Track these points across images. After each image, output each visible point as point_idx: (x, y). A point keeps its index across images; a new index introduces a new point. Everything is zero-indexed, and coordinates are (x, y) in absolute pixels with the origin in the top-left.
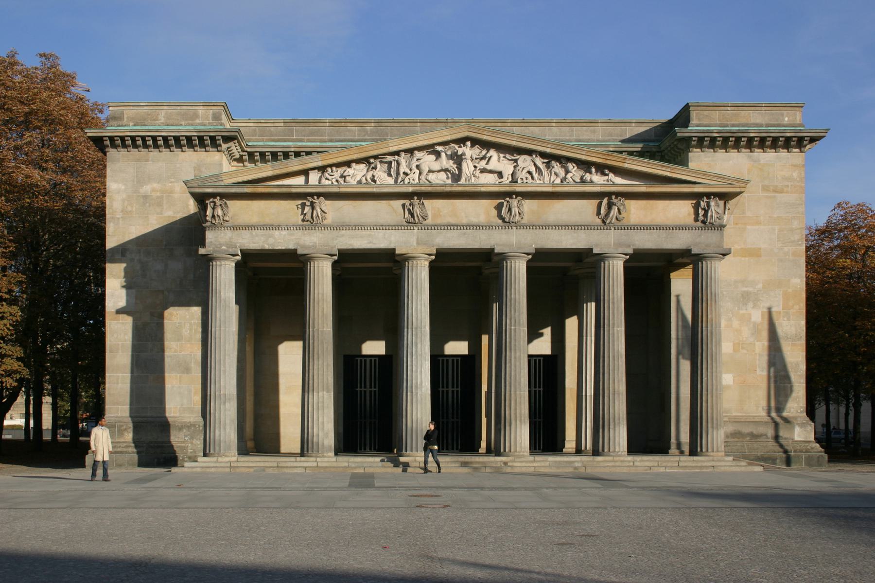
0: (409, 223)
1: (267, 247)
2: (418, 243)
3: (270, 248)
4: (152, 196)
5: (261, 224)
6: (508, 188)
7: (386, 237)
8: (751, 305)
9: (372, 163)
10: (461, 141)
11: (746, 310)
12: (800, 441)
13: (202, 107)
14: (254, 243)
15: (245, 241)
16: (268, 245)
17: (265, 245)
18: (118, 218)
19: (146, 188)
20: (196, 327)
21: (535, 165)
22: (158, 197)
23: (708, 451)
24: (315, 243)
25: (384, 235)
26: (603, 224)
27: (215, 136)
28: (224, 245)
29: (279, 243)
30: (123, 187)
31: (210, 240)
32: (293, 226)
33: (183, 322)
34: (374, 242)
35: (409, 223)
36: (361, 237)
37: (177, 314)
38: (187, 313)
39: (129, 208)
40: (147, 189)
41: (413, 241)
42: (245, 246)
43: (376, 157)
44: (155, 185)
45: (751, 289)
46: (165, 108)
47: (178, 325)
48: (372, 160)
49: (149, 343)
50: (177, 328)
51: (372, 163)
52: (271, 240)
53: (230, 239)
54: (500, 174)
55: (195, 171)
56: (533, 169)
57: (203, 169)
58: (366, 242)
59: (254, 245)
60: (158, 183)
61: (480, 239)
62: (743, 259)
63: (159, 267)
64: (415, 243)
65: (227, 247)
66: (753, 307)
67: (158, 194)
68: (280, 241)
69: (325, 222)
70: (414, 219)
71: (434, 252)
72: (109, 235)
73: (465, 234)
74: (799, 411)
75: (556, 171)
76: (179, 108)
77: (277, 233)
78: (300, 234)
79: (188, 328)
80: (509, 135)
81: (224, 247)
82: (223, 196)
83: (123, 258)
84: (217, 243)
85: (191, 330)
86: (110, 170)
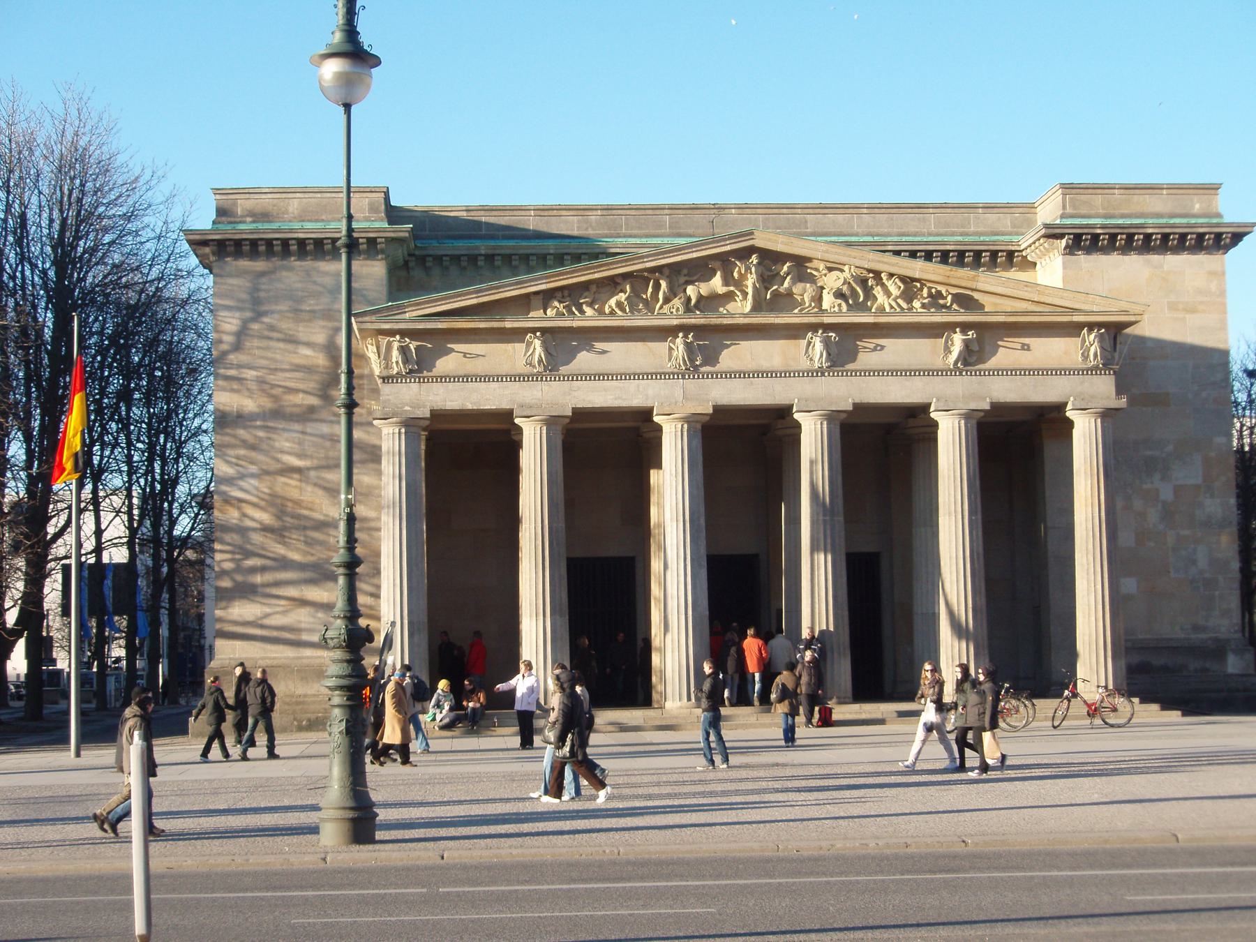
1: (470, 407)
5: (462, 373)
7: (641, 389)
8: (1157, 476)
9: (619, 284)
10: (744, 254)
11: (1152, 483)
12: (1236, 675)
14: (451, 401)
15: (438, 398)
24: (539, 399)
27: (376, 238)
28: (407, 405)
34: (624, 397)
41: (679, 394)
46: (298, 195)
48: (619, 280)
51: (619, 284)
59: (450, 403)
62: (1144, 409)
65: (411, 407)
66: (1162, 479)
71: (711, 411)
74: (1232, 631)
76: (319, 195)
78: (517, 387)
81: (407, 408)
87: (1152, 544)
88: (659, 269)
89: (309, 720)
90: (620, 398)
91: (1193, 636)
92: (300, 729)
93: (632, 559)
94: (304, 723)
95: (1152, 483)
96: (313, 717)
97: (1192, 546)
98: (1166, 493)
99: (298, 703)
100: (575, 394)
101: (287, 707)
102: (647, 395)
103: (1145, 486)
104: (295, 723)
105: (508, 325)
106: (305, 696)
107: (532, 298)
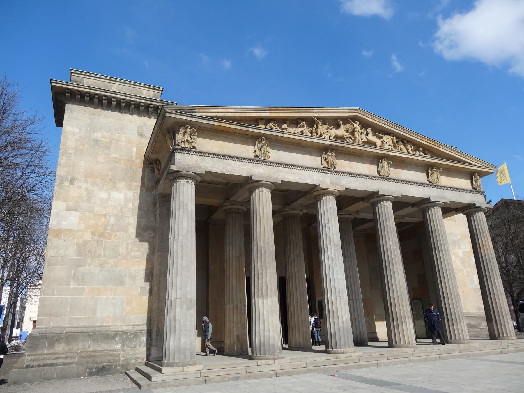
0: (325, 168)
1: (226, 172)
2: (331, 183)
3: (228, 173)
4: (102, 141)
6: (385, 152)
7: (311, 176)
8: (457, 248)
10: (354, 119)
13: (145, 89)
14: (215, 168)
16: (227, 171)
17: (225, 171)
18: (70, 154)
19: (97, 134)
20: (131, 246)
21: (393, 141)
22: (106, 142)
23: (507, 336)
24: (262, 174)
25: (309, 174)
26: (431, 184)
29: (235, 170)
30: (78, 131)
31: (179, 160)
32: (246, 159)
33: (121, 242)
35: (325, 168)
36: (294, 174)
37: (116, 235)
38: (125, 235)
39: (81, 147)
40: (98, 135)
41: (328, 181)
42: (208, 169)
43: (303, 119)
44: (105, 134)
45: (455, 239)
47: (116, 243)
49: (88, 258)
50: (115, 246)
52: (229, 167)
53: (196, 162)
54: (375, 144)
55: (138, 129)
56: (391, 143)
57: (145, 129)
58: (298, 178)
59: (215, 169)
60: (108, 132)
61: (367, 184)
62: (449, 222)
63: (103, 195)
64: (329, 183)
66: (459, 249)
67: (108, 140)
68: (236, 169)
69: (269, 160)
70: (329, 166)
72: (60, 166)
73: (358, 180)
75: (401, 147)
76: (128, 85)
77: (233, 162)
79: (125, 246)
80: (381, 120)
82: (192, 125)
83: (71, 185)
84: (185, 164)
85: (127, 248)
86: (68, 116)
87: (460, 274)
88: (319, 118)
89: (97, 368)
90: (300, 178)
91: (479, 312)
92: (91, 374)
93: (250, 277)
94: (94, 370)
95: (456, 250)
96: (101, 365)
97: (472, 275)
98: (461, 254)
99: (91, 357)
100: (280, 173)
101: (82, 360)
102: (314, 180)
103: (454, 251)
104: (88, 370)
105: (250, 130)
106: (95, 351)
107: (260, 121)
